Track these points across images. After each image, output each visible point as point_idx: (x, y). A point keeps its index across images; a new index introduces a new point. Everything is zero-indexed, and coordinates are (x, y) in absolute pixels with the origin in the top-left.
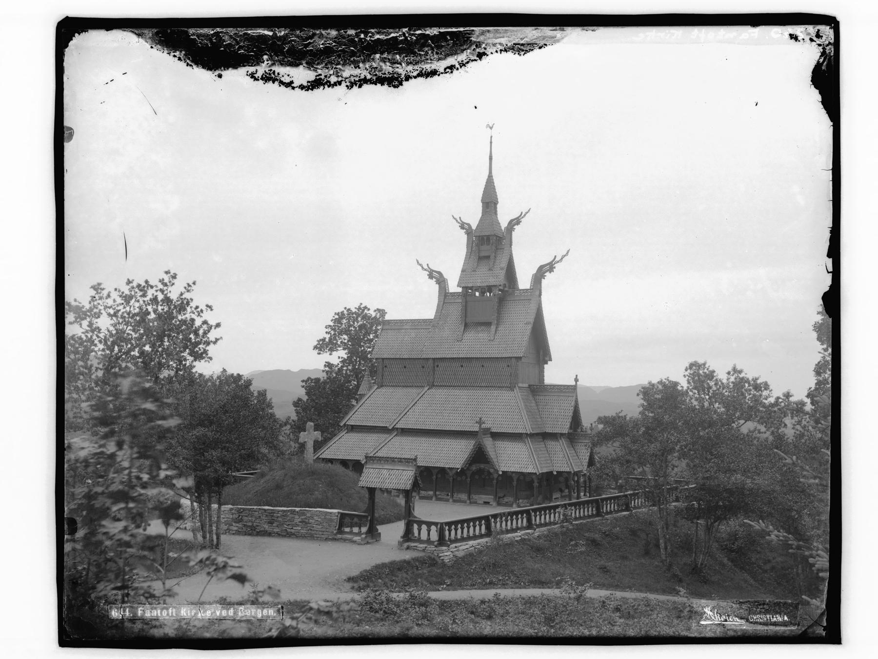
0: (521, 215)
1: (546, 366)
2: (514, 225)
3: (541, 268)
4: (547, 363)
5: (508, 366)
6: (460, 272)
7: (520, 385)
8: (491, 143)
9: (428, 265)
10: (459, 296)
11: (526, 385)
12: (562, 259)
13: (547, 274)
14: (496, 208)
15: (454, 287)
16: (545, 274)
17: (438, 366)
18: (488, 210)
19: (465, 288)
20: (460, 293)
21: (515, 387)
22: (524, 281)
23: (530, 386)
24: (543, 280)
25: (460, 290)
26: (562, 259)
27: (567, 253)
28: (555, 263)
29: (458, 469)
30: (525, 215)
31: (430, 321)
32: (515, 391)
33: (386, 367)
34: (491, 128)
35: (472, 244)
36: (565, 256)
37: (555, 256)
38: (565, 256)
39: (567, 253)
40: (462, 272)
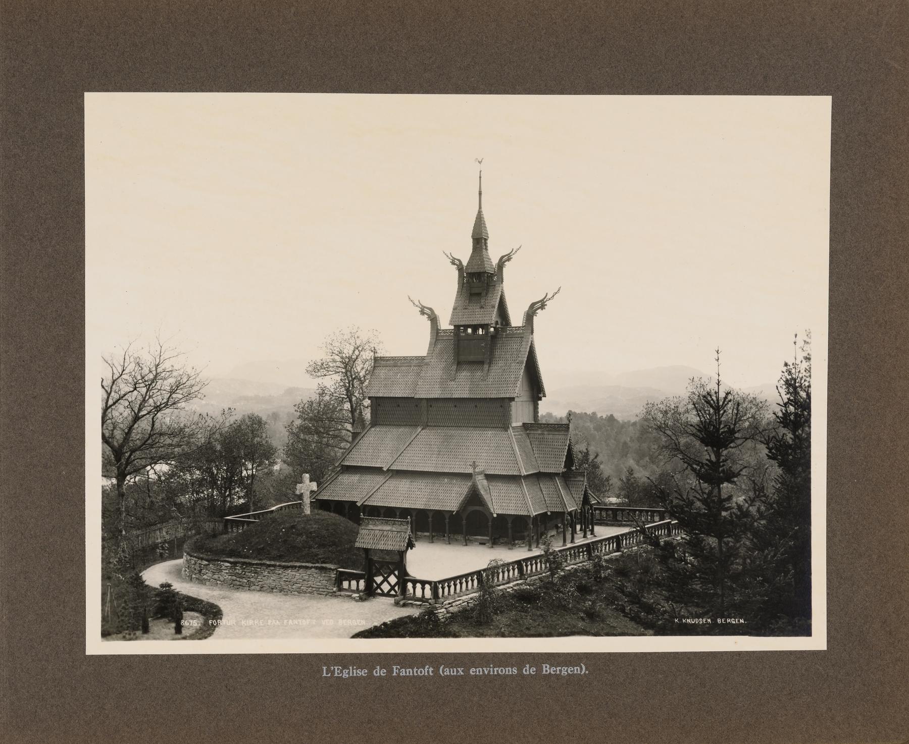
0: (513, 250)
1: (539, 402)
2: (505, 262)
3: (533, 305)
4: (540, 399)
5: (501, 406)
6: (452, 310)
7: (514, 425)
8: (480, 177)
9: (419, 301)
10: (451, 332)
11: (520, 424)
12: (553, 296)
13: (539, 311)
14: (486, 244)
15: (445, 324)
16: (537, 312)
17: (431, 406)
18: (478, 246)
19: (457, 327)
20: (452, 330)
21: (508, 427)
22: (516, 319)
23: (523, 424)
24: (534, 317)
25: (452, 327)
26: (553, 296)
27: (559, 290)
28: (546, 301)
29: (454, 511)
30: (516, 251)
31: (423, 358)
32: (509, 431)
33: (379, 405)
34: (480, 162)
35: (464, 280)
36: (556, 293)
37: (547, 294)
38: (556, 293)
39: (559, 290)
40: (454, 309)
